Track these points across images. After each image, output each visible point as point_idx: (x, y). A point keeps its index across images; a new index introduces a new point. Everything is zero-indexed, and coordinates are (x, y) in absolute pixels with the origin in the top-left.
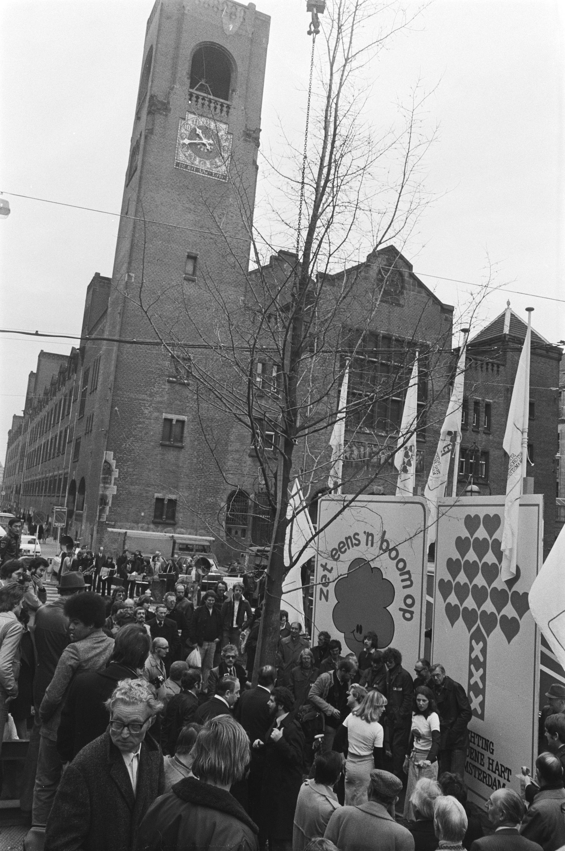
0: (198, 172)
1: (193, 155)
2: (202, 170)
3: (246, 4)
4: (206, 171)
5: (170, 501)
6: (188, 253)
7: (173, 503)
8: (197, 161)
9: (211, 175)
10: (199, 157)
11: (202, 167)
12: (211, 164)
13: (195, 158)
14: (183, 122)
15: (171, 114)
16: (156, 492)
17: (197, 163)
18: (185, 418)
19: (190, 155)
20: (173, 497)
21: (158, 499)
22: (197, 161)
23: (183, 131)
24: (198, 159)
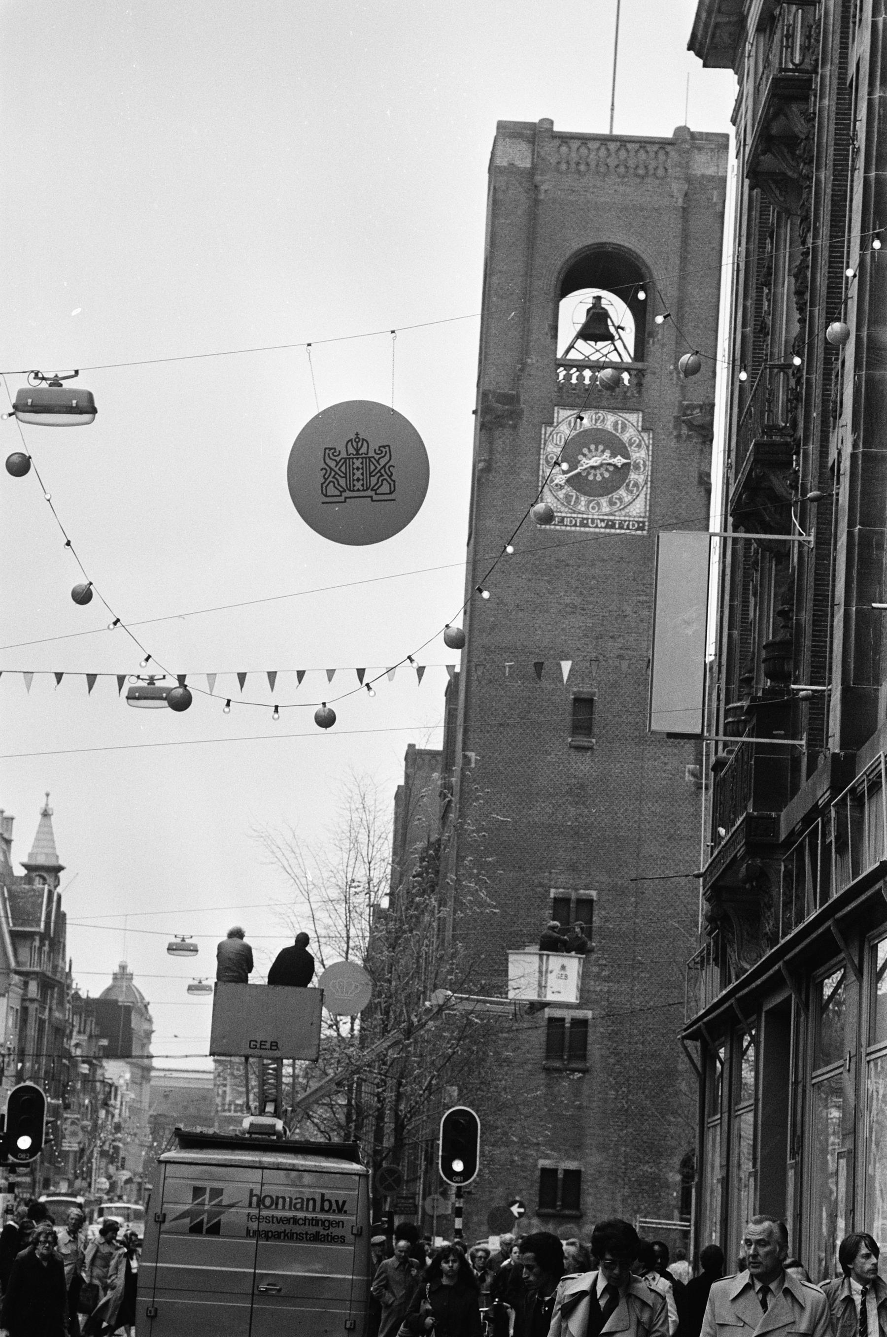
0: (586, 526)
1: (574, 493)
2: (593, 520)
3: (669, 134)
4: (602, 520)
5: (567, 1172)
6: (574, 693)
7: (574, 1176)
8: (583, 503)
9: (613, 526)
10: (585, 494)
11: (594, 514)
12: (611, 503)
13: (577, 498)
14: (549, 429)
15: (524, 423)
16: (541, 1158)
17: (583, 509)
18: (589, 1014)
19: (568, 497)
20: (572, 1165)
21: (544, 1170)
22: (583, 503)
23: (550, 448)
24: (583, 499)
